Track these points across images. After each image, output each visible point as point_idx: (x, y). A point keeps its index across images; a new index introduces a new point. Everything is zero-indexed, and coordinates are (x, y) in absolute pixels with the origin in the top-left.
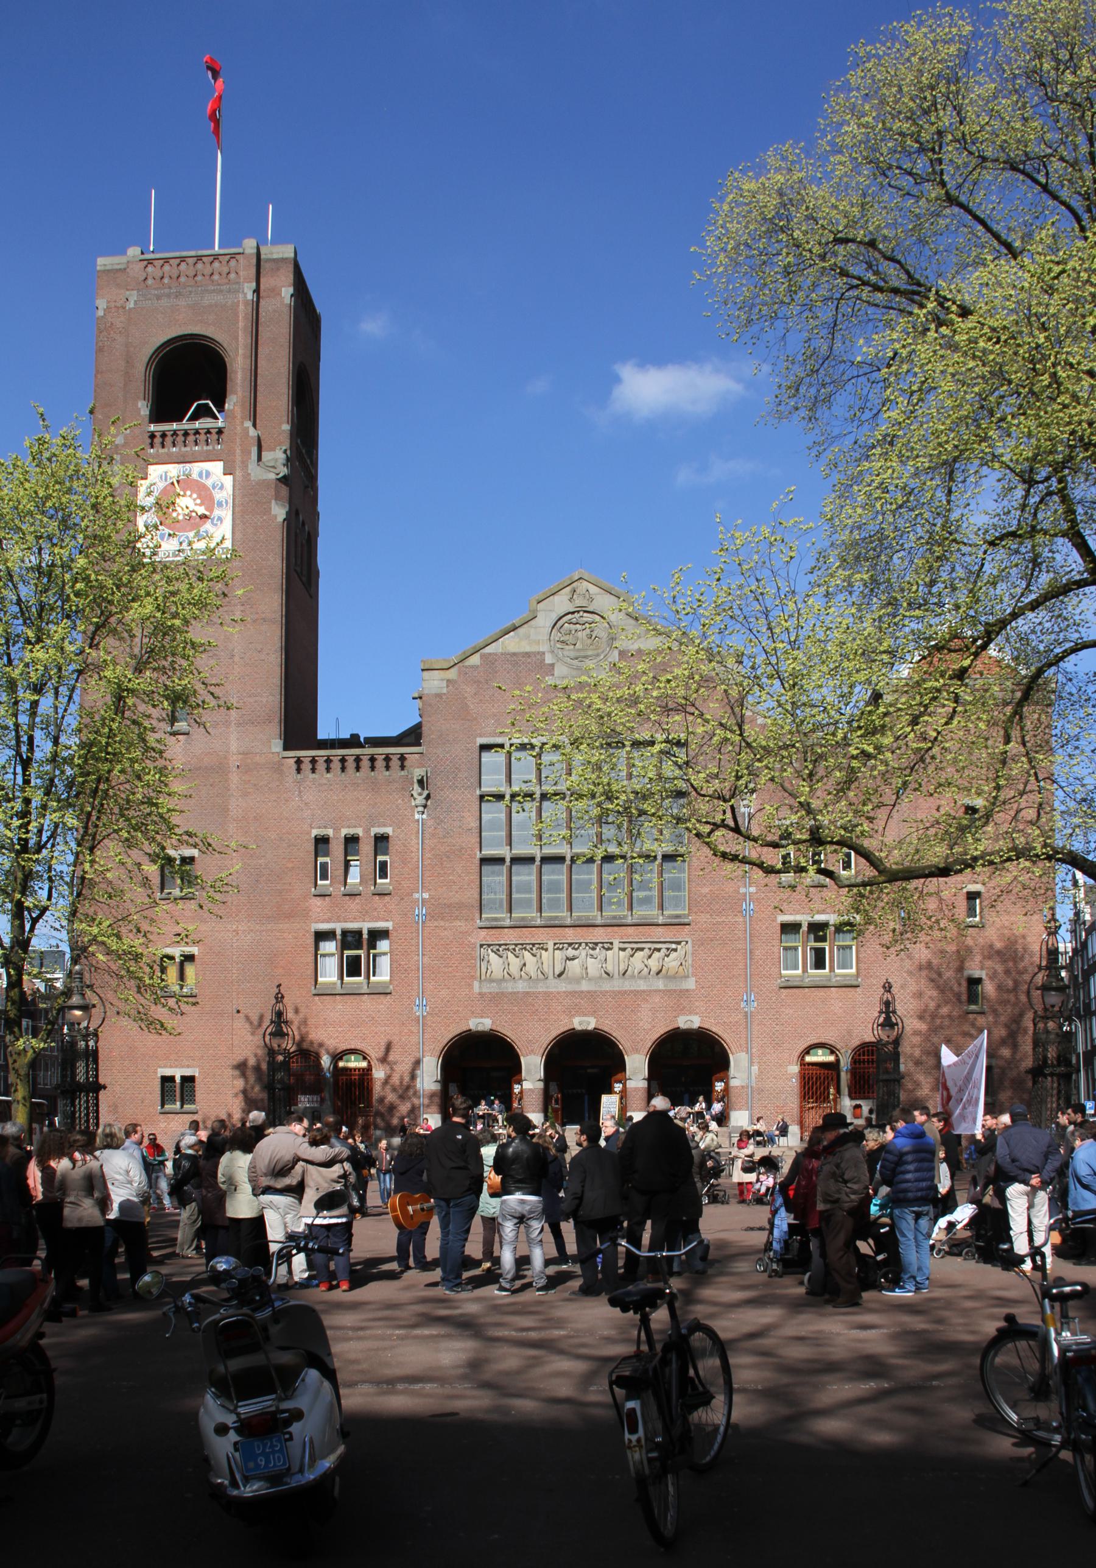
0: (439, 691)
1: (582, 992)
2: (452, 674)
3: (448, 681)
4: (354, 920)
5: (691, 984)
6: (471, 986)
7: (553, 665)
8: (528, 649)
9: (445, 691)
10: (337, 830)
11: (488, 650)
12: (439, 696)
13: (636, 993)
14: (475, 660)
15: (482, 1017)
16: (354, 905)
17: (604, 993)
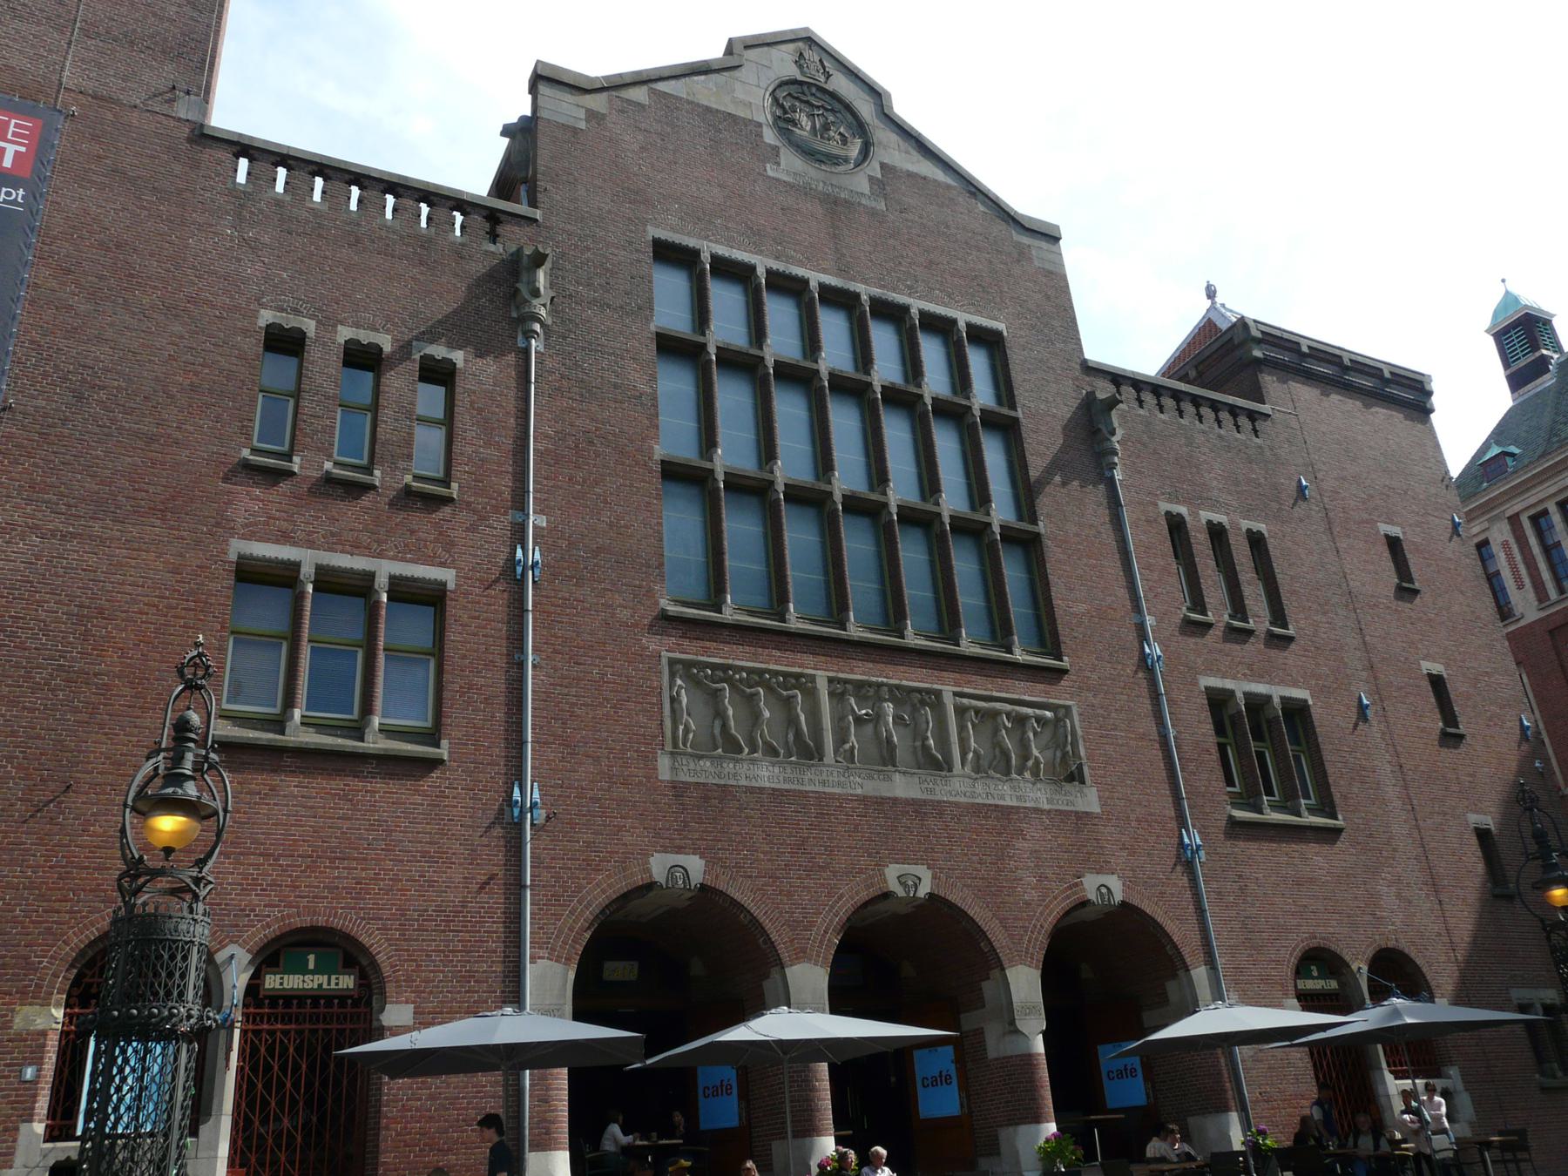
0: (571, 122)
1: (895, 800)
2: (597, 102)
3: (588, 110)
4: (356, 548)
5: (1088, 800)
6: (649, 760)
7: (776, 149)
8: (731, 109)
9: (582, 125)
10: (328, 323)
11: (661, 86)
12: (575, 131)
13: (1006, 812)
14: (639, 94)
15: (679, 850)
16: (351, 514)
17: (939, 808)
